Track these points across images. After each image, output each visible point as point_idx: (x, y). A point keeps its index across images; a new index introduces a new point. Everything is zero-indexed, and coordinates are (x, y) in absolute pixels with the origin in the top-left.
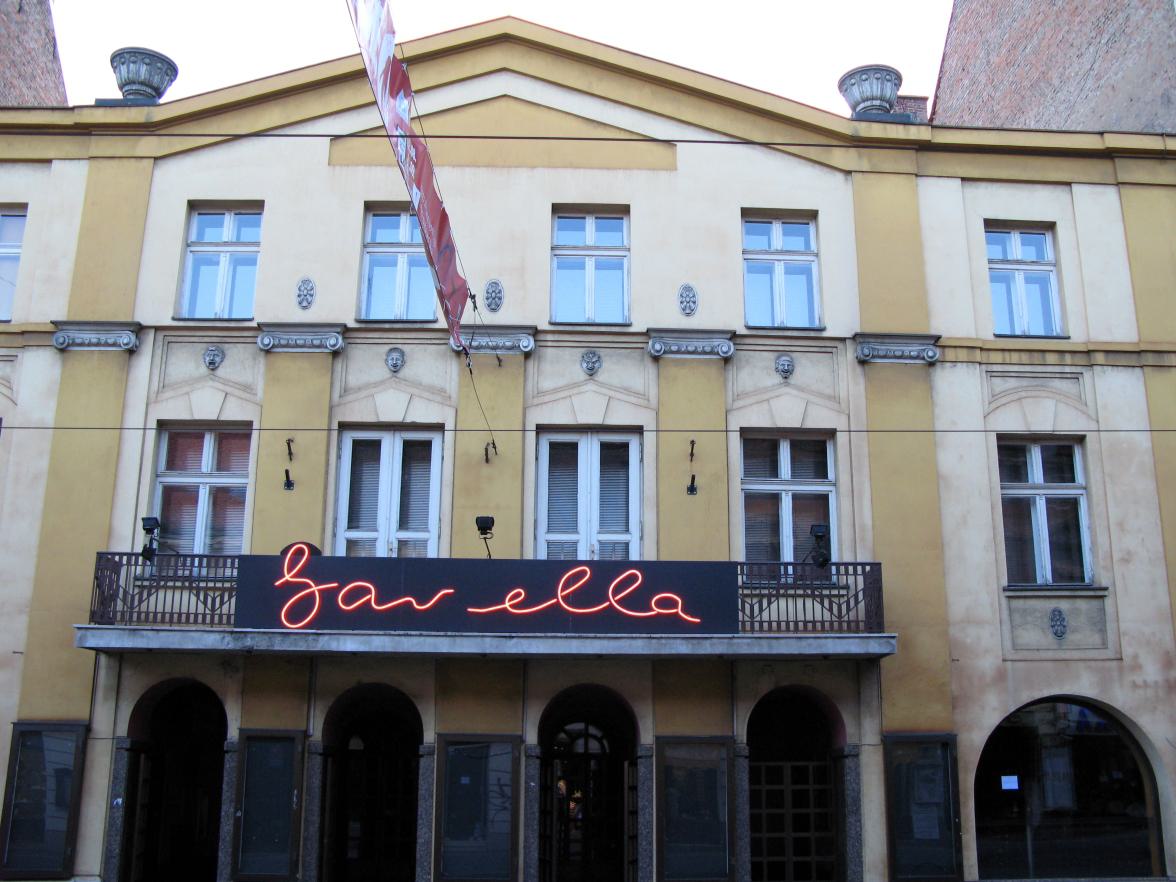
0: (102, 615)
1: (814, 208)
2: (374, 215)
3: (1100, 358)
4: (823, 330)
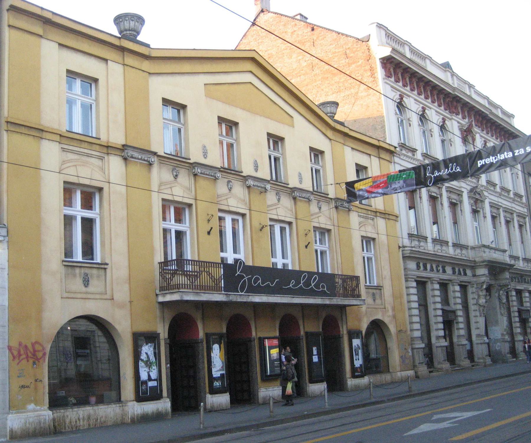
0: (166, 288)
1: (284, 137)
2: (172, 108)
3: (378, 214)
4: (288, 184)
